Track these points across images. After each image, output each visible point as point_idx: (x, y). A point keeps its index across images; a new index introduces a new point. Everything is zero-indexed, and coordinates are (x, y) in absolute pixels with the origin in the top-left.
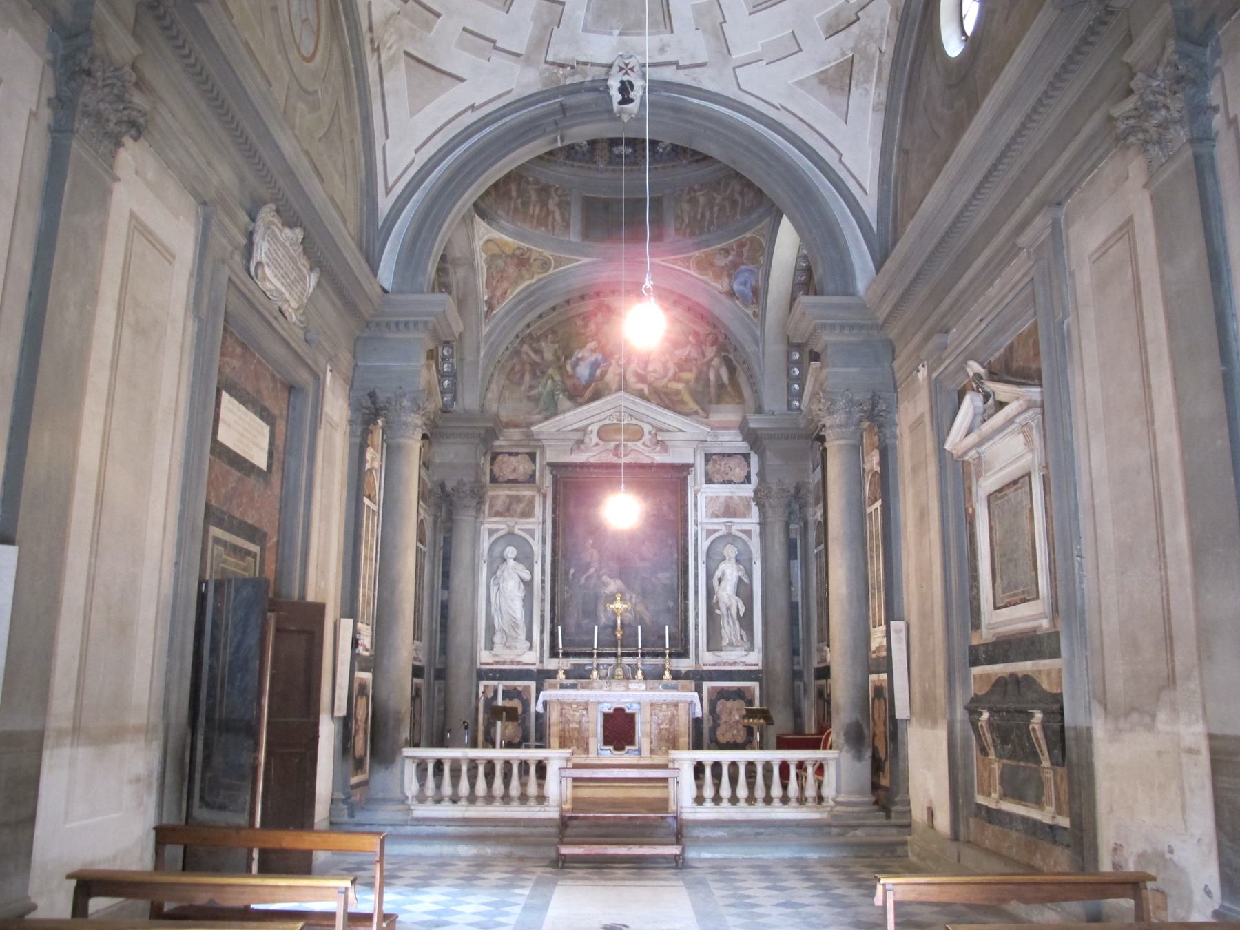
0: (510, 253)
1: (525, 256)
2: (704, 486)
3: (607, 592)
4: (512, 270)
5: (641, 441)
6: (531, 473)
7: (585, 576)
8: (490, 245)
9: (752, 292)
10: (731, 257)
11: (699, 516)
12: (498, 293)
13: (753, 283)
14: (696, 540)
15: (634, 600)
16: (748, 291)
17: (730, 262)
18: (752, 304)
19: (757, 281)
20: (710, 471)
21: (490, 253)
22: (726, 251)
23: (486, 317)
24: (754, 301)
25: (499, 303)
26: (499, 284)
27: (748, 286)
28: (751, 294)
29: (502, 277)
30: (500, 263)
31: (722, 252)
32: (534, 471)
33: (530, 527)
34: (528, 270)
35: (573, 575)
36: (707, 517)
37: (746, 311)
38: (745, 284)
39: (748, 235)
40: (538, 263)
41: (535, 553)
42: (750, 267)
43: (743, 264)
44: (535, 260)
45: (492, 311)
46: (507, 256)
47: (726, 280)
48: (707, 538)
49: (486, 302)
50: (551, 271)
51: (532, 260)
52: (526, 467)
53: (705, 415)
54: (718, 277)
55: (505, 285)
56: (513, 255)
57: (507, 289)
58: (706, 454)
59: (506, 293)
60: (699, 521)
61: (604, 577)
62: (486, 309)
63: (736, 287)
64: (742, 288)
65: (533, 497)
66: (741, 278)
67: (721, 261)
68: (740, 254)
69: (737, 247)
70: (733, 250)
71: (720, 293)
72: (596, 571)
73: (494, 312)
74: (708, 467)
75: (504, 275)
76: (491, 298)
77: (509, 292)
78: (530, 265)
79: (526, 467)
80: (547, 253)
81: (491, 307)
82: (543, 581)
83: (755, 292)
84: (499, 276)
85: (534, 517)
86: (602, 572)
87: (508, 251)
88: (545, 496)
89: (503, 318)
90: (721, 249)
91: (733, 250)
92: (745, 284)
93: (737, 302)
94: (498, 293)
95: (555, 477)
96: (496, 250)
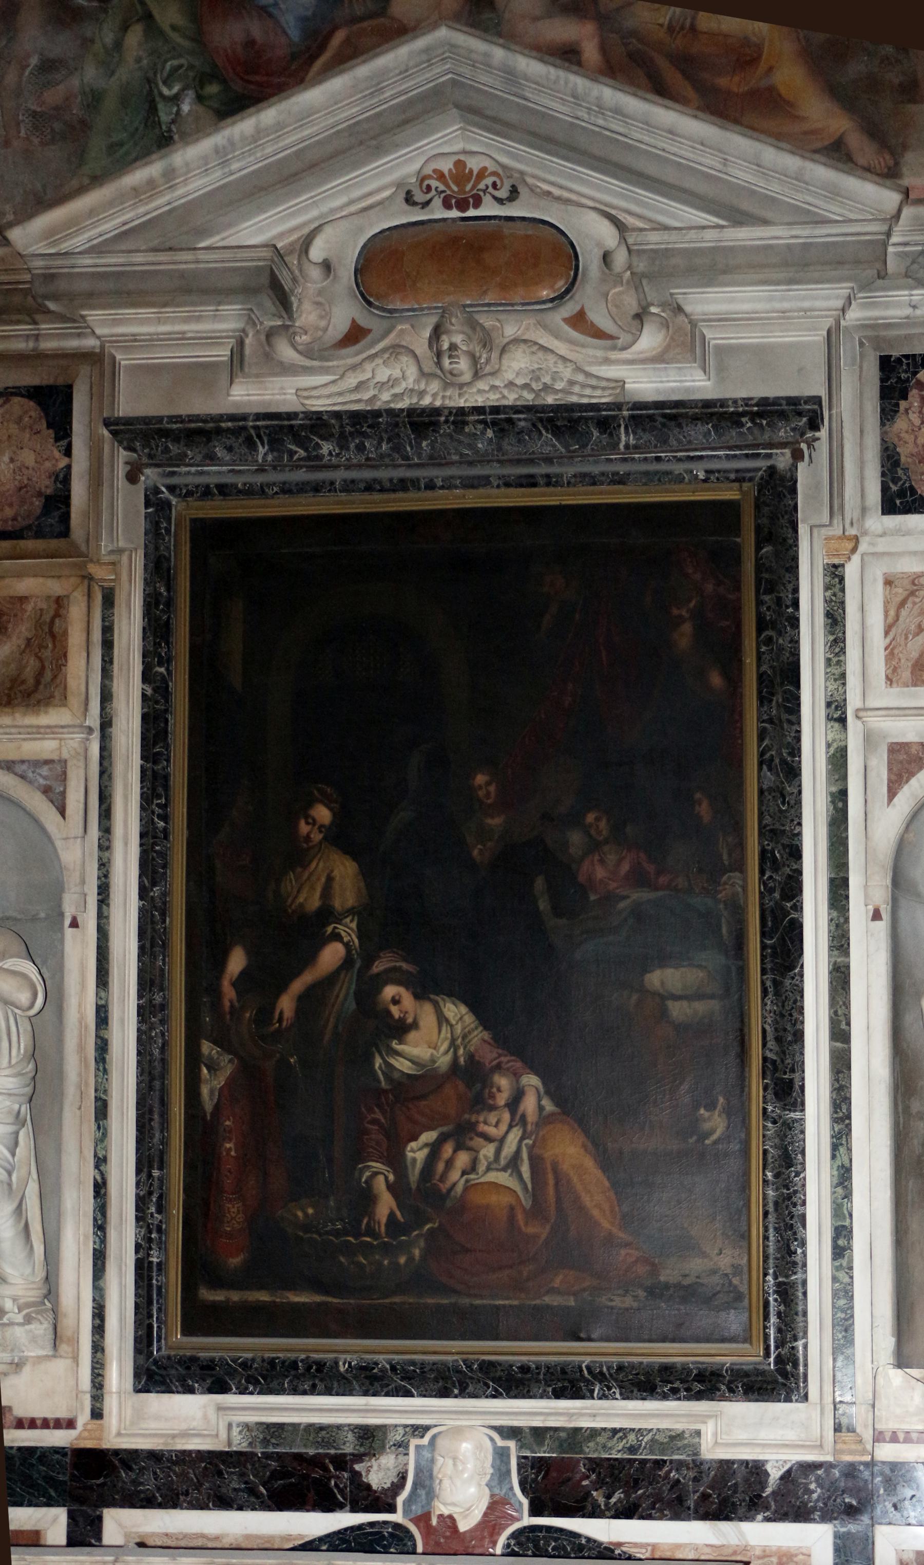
2: (878, 522)
3: (403, 1065)
5: (569, 309)
6: (47, 485)
7: (298, 986)
11: (853, 681)
14: (840, 798)
15: (529, 1104)
20: (905, 452)
32: (64, 478)
33: (46, 748)
35: (244, 981)
36: (889, 680)
41: (72, 881)
48: (892, 794)
52: (28, 457)
53: (884, 161)
58: (887, 364)
60: (853, 701)
61: (390, 991)
65: (60, 603)
72: (347, 963)
74: (900, 424)
79: (28, 457)
82: (102, 1017)
85: (64, 701)
86: (378, 967)
88: (109, 601)
95: (152, 499)
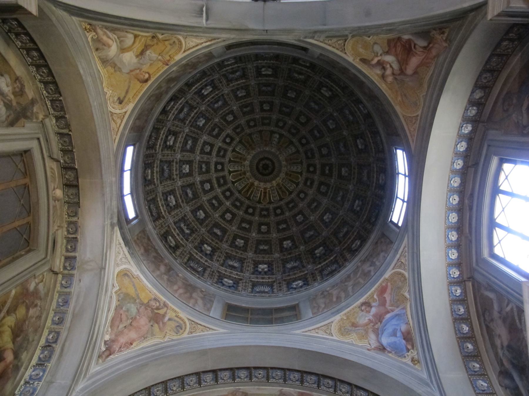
0: (146, 301)
1: (162, 312)
4: (143, 321)
8: (126, 281)
9: (404, 339)
10: (374, 310)
12: (122, 340)
13: (404, 328)
16: (399, 340)
17: (374, 316)
18: (408, 350)
19: (408, 323)
21: (124, 290)
22: (367, 304)
23: (100, 356)
24: (409, 347)
25: (120, 350)
26: (126, 331)
27: (399, 334)
28: (404, 341)
29: (131, 324)
30: (133, 309)
31: (363, 308)
34: (160, 329)
37: (404, 360)
38: (394, 334)
39: (387, 275)
40: (173, 324)
42: (397, 311)
43: (388, 312)
44: (170, 319)
45: (110, 355)
46: (142, 304)
47: (372, 337)
49: (105, 342)
50: (185, 335)
51: (166, 319)
54: (364, 336)
55: (133, 335)
56: (147, 306)
57: (134, 340)
59: (131, 344)
62: (103, 349)
63: (385, 340)
64: (393, 339)
66: (390, 329)
67: (364, 318)
68: (383, 303)
69: (378, 296)
70: (375, 300)
71: (368, 350)
73: (112, 356)
75: (134, 324)
76: (113, 341)
77: (134, 344)
78: (164, 324)
80: (182, 315)
81: (109, 351)
83: (408, 337)
84: (129, 321)
87: (144, 297)
89: (121, 362)
90: (363, 304)
91: (375, 300)
92: (394, 334)
93: (390, 355)
94: (122, 340)
96: (132, 291)
